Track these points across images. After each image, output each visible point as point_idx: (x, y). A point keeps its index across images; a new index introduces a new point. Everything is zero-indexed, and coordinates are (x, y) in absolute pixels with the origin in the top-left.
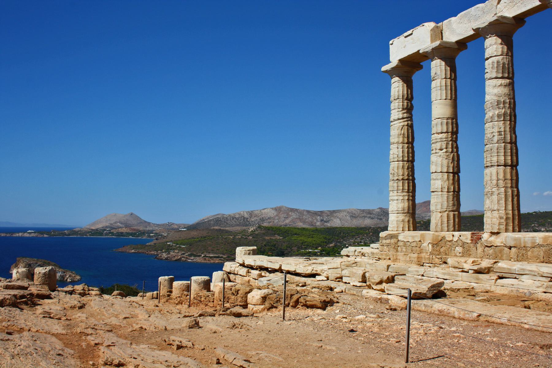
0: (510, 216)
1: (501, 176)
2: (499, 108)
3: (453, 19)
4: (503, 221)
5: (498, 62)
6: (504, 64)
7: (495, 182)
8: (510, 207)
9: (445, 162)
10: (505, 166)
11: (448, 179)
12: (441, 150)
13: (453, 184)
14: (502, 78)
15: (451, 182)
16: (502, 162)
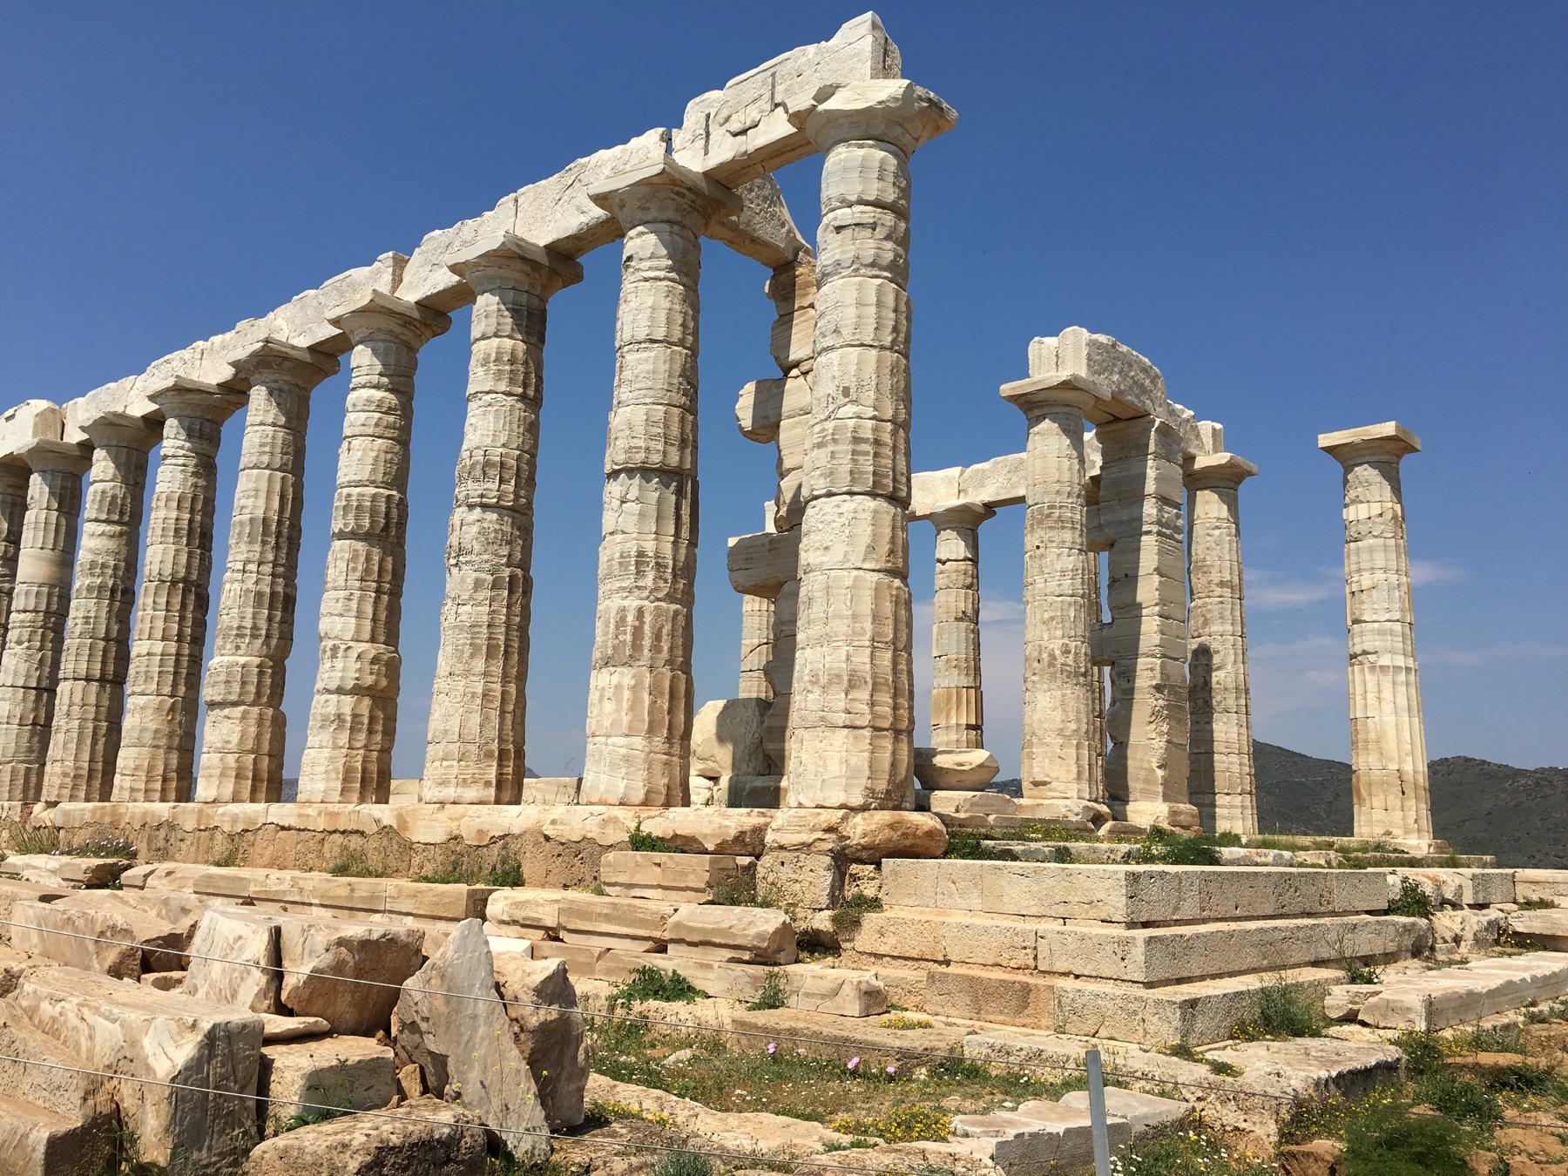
0: (85, 773)
1: (77, 698)
2: (92, 575)
3: (80, 400)
4: (68, 780)
5: (103, 492)
6: (114, 497)
7: (65, 708)
8: (86, 756)
9: (23, 667)
10: (88, 679)
11: (24, 700)
12: (19, 643)
13: (36, 709)
14: (107, 521)
15: (30, 705)
16: (83, 674)
